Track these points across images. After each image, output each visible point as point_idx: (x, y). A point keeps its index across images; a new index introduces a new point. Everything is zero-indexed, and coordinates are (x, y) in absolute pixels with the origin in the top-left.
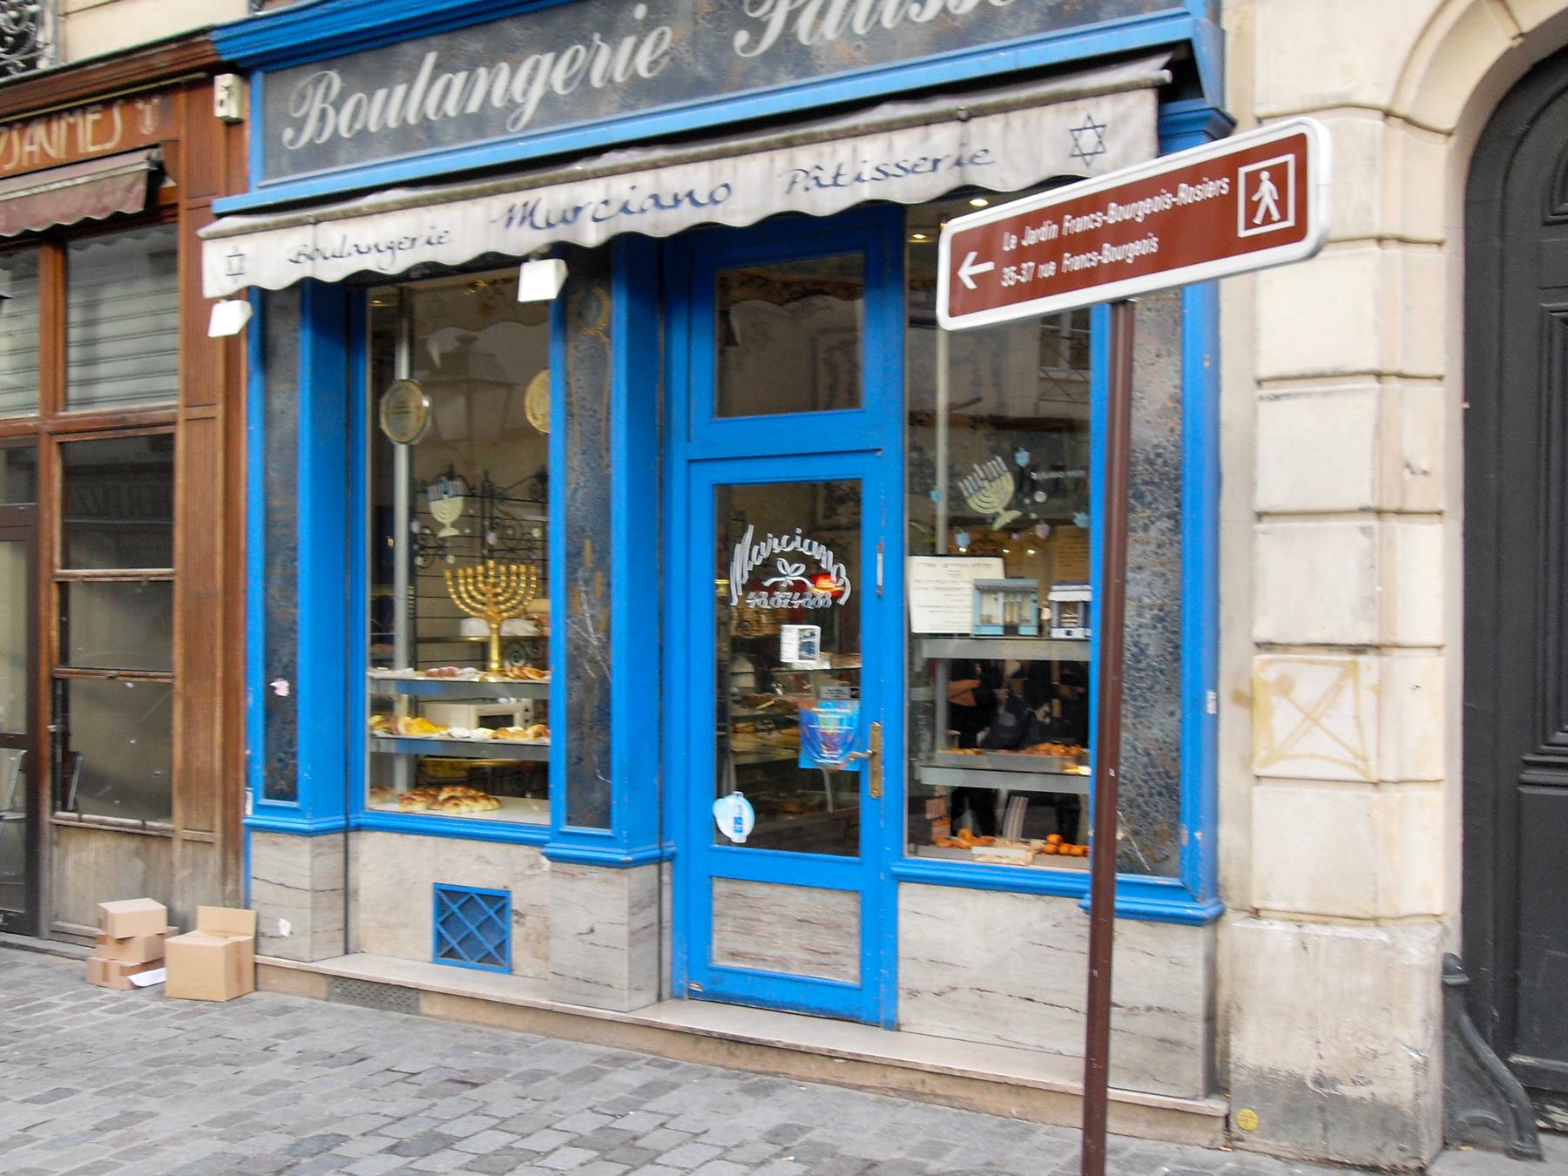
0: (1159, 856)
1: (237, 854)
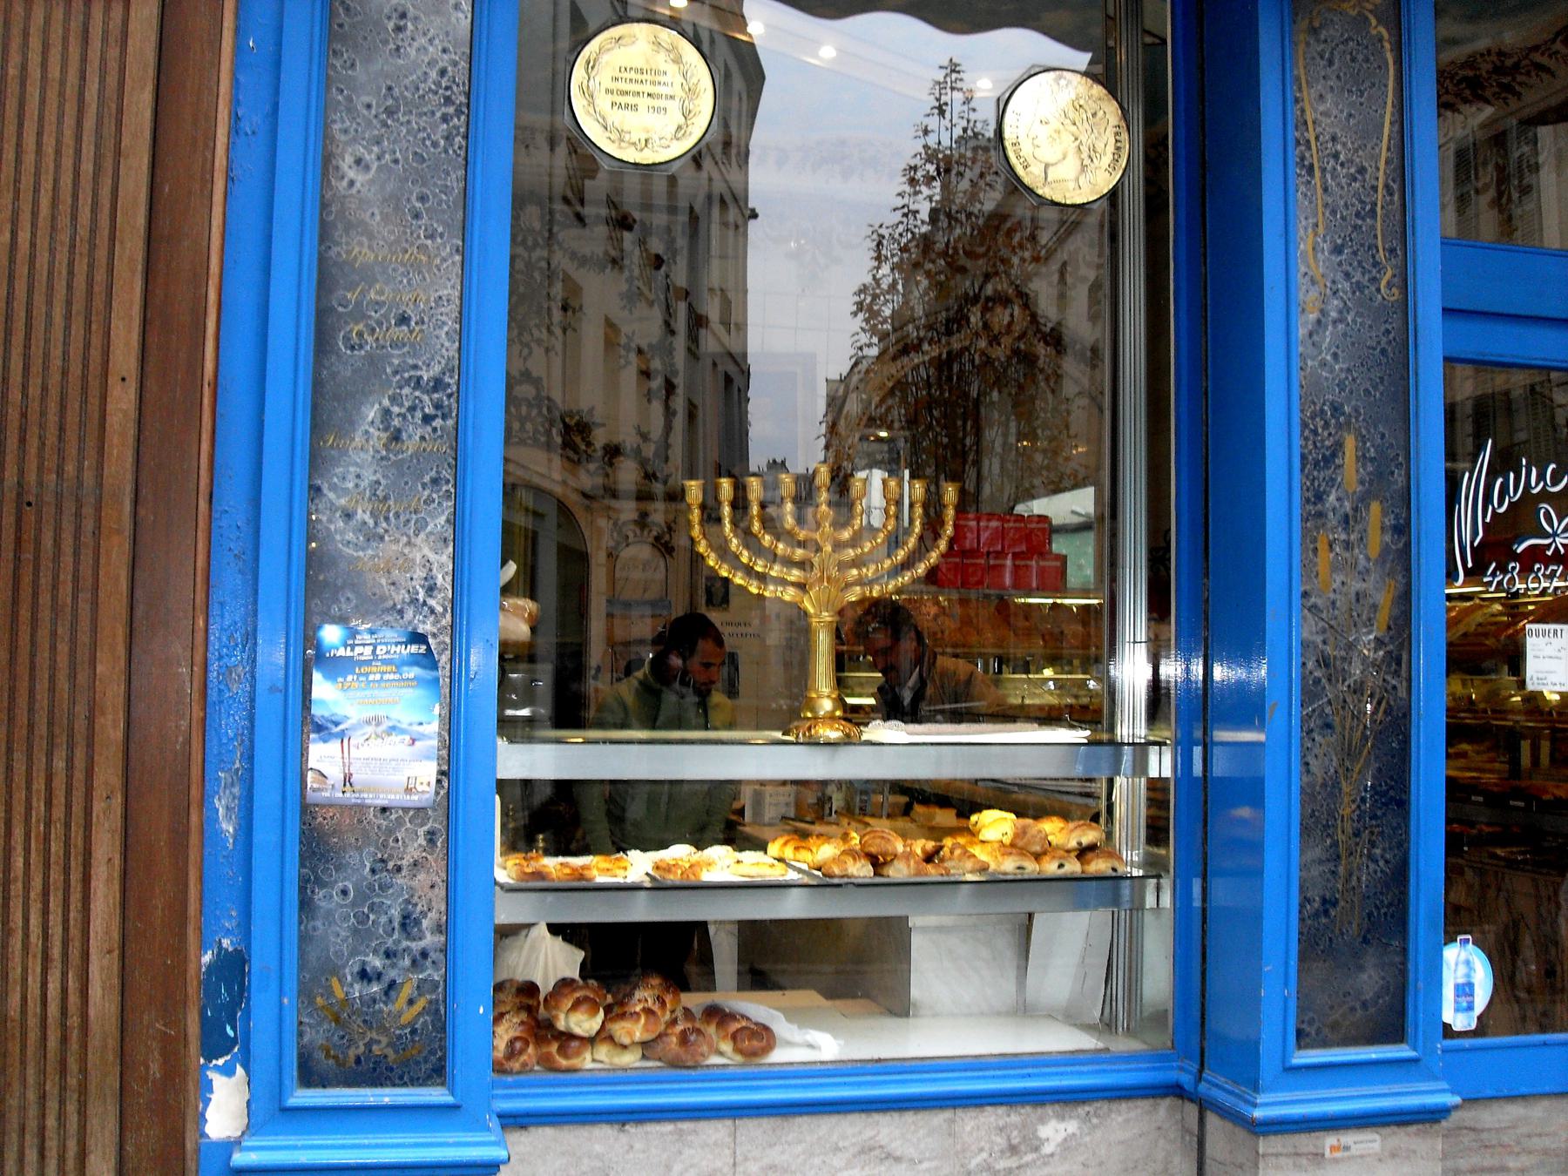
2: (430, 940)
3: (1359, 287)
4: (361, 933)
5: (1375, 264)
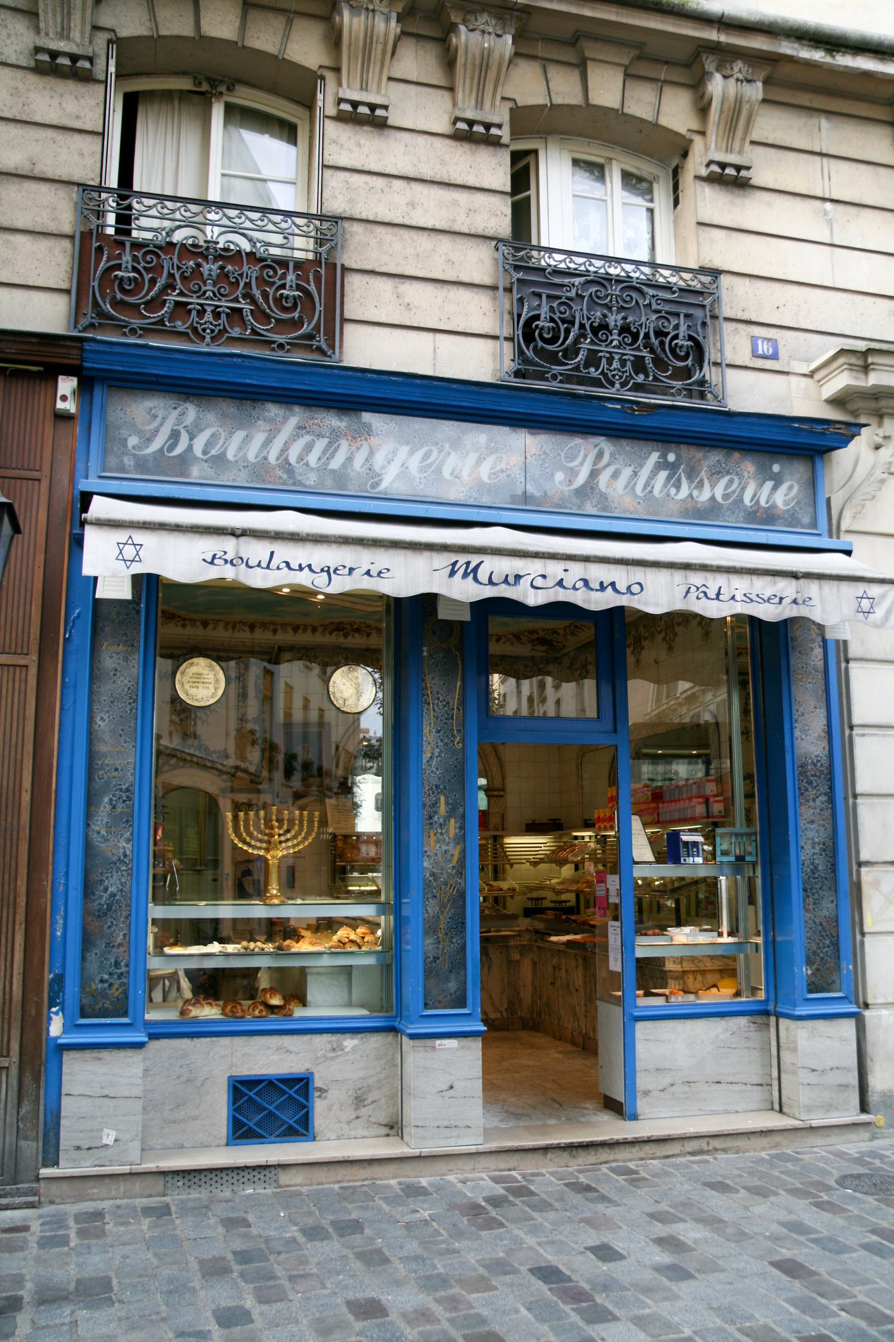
0: (830, 981)
1: (37, 1078)
2: (123, 969)
3: (446, 744)
4: (101, 968)
5: (453, 735)
